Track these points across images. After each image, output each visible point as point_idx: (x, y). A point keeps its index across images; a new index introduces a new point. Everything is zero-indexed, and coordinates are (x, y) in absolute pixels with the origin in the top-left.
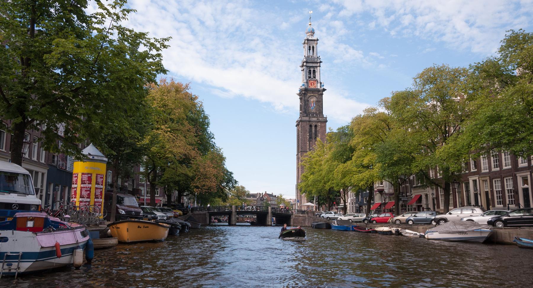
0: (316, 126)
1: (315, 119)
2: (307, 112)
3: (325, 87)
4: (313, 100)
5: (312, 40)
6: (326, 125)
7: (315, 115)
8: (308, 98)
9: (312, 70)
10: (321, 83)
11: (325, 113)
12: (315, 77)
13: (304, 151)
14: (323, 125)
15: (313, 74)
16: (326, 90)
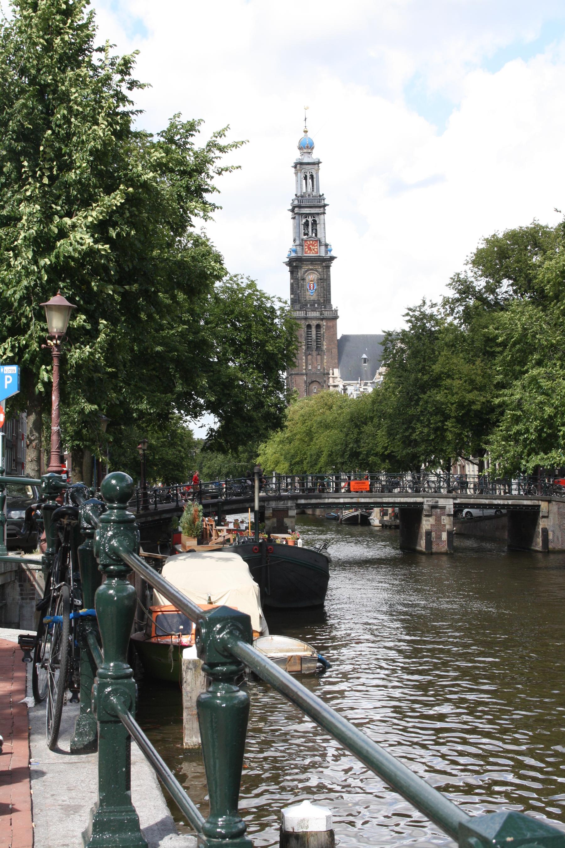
0: (318, 327)
1: (316, 314)
2: (303, 300)
3: (333, 254)
4: (312, 277)
5: (308, 164)
6: (336, 324)
7: (316, 306)
8: (304, 274)
9: (310, 220)
10: (326, 245)
11: (336, 301)
12: (316, 235)
13: (297, 374)
14: (330, 324)
15: (312, 224)
16: (336, 258)
